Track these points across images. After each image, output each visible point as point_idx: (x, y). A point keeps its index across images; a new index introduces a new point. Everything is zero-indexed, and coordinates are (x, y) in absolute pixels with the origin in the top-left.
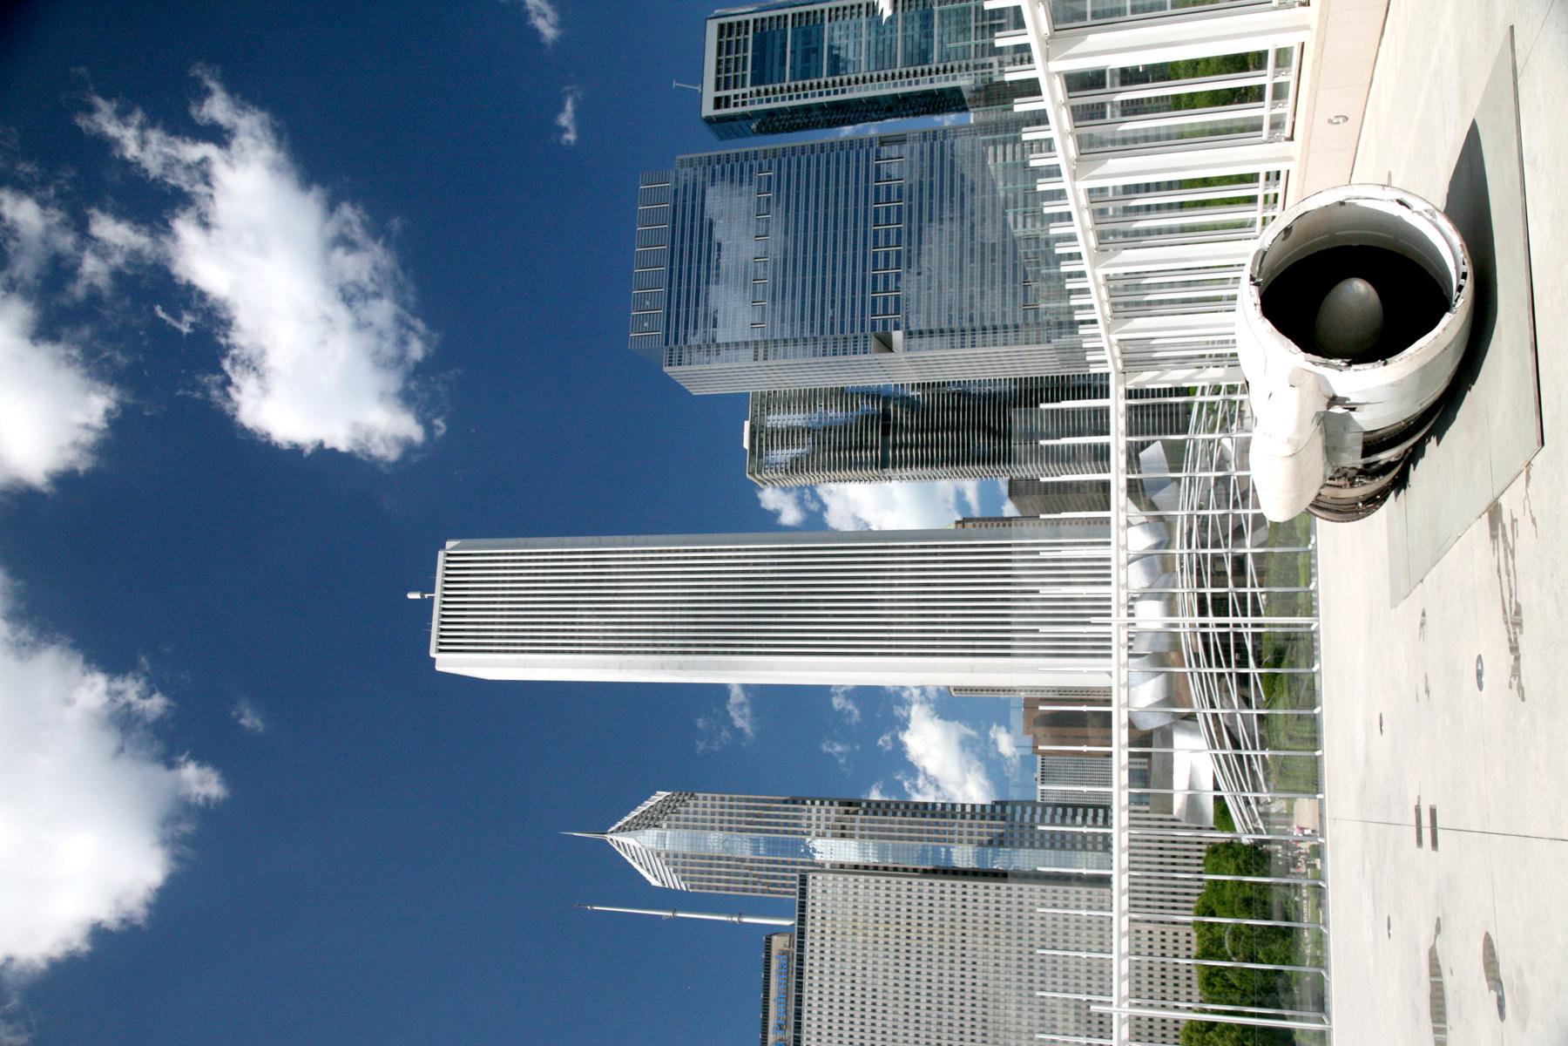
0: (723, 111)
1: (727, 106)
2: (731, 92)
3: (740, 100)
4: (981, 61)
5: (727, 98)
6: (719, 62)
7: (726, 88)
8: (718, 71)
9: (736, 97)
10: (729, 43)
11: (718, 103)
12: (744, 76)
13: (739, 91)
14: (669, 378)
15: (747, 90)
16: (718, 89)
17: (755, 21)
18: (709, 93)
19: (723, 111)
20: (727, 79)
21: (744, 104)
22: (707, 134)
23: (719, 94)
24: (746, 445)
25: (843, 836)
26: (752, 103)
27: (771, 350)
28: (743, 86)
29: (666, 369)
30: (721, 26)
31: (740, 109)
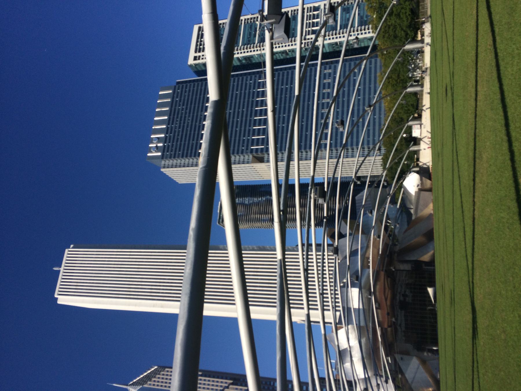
0: (197, 62)
1: (199, 59)
4: (308, 37)
5: (200, 56)
6: (197, 42)
7: (199, 52)
8: (197, 45)
11: (195, 58)
14: (165, 174)
16: (196, 52)
19: (197, 62)
20: (200, 49)
22: (191, 72)
24: (219, 212)
29: (162, 170)
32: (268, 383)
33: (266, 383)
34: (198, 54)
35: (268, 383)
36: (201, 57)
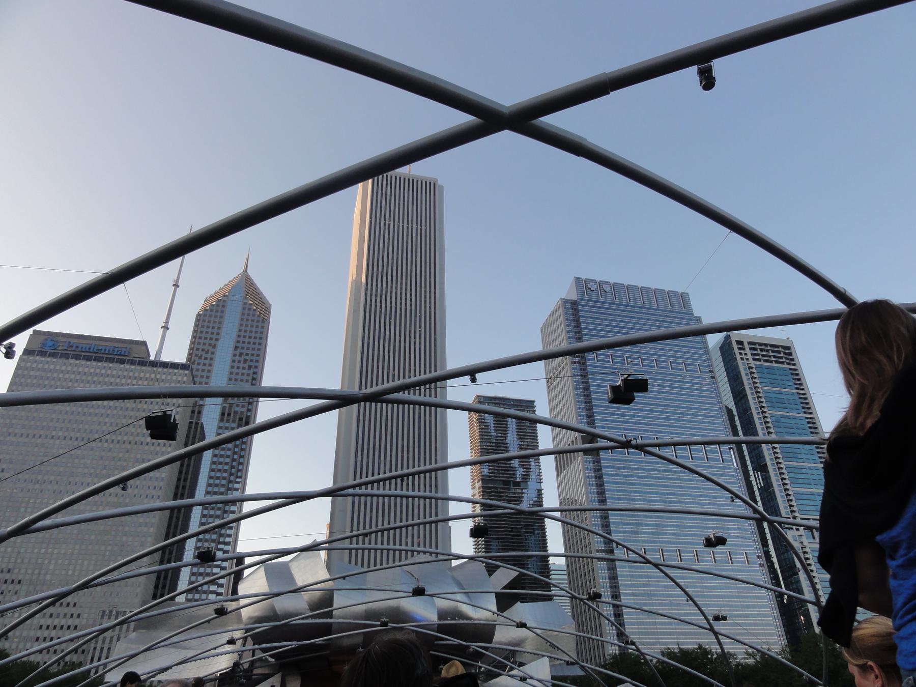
0: (735, 346)
1: (739, 348)
2: (748, 351)
5: (744, 349)
7: (751, 349)
10: (779, 352)
11: (740, 343)
12: (759, 360)
13: (750, 357)
16: (749, 343)
19: (735, 346)
20: (756, 349)
21: (742, 359)
25: (223, 414)
26: (744, 364)
27: (578, 366)
28: (754, 359)
31: (738, 357)
32: (239, 474)
33: (239, 471)
34: (747, 346)
35: (239, 474)
36: (743, 352)
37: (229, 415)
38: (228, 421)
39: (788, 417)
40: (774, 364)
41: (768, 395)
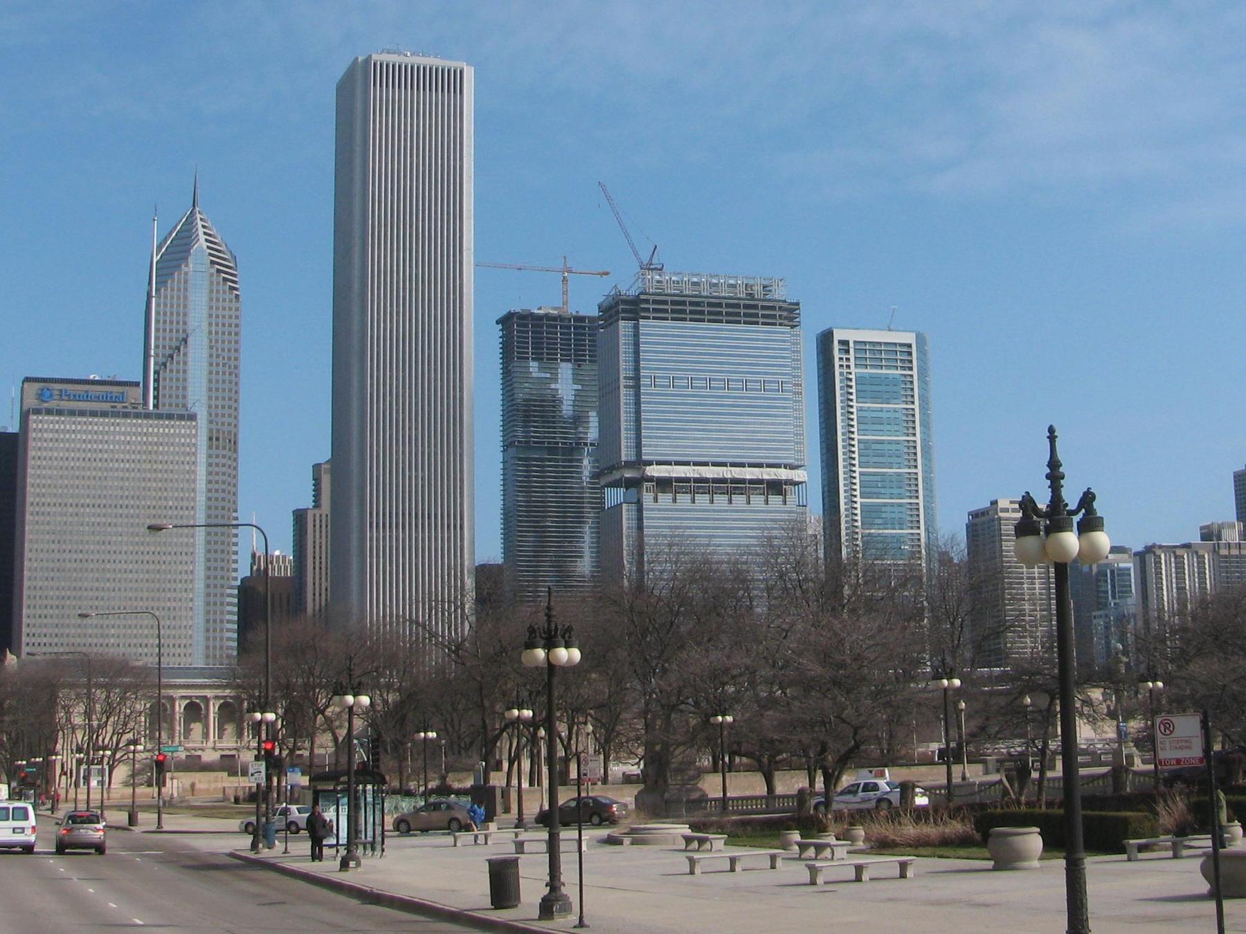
3: (845, 363)
5: (847, 352)
9: (848, 359)
11: (844, 343)
13: (852, 363)
15: (853, 369)
16: (855, 342)
17: (912, 376)
18: (852, 336)
23: (851, 345)
25: (211, 439)
26: (841, 374)
30: (910, 346)
31: (837, 363)
37: (217, 439)
38: (217, 448)
39: (881, 442)
40: (884, 371)
41: (864, 414)
